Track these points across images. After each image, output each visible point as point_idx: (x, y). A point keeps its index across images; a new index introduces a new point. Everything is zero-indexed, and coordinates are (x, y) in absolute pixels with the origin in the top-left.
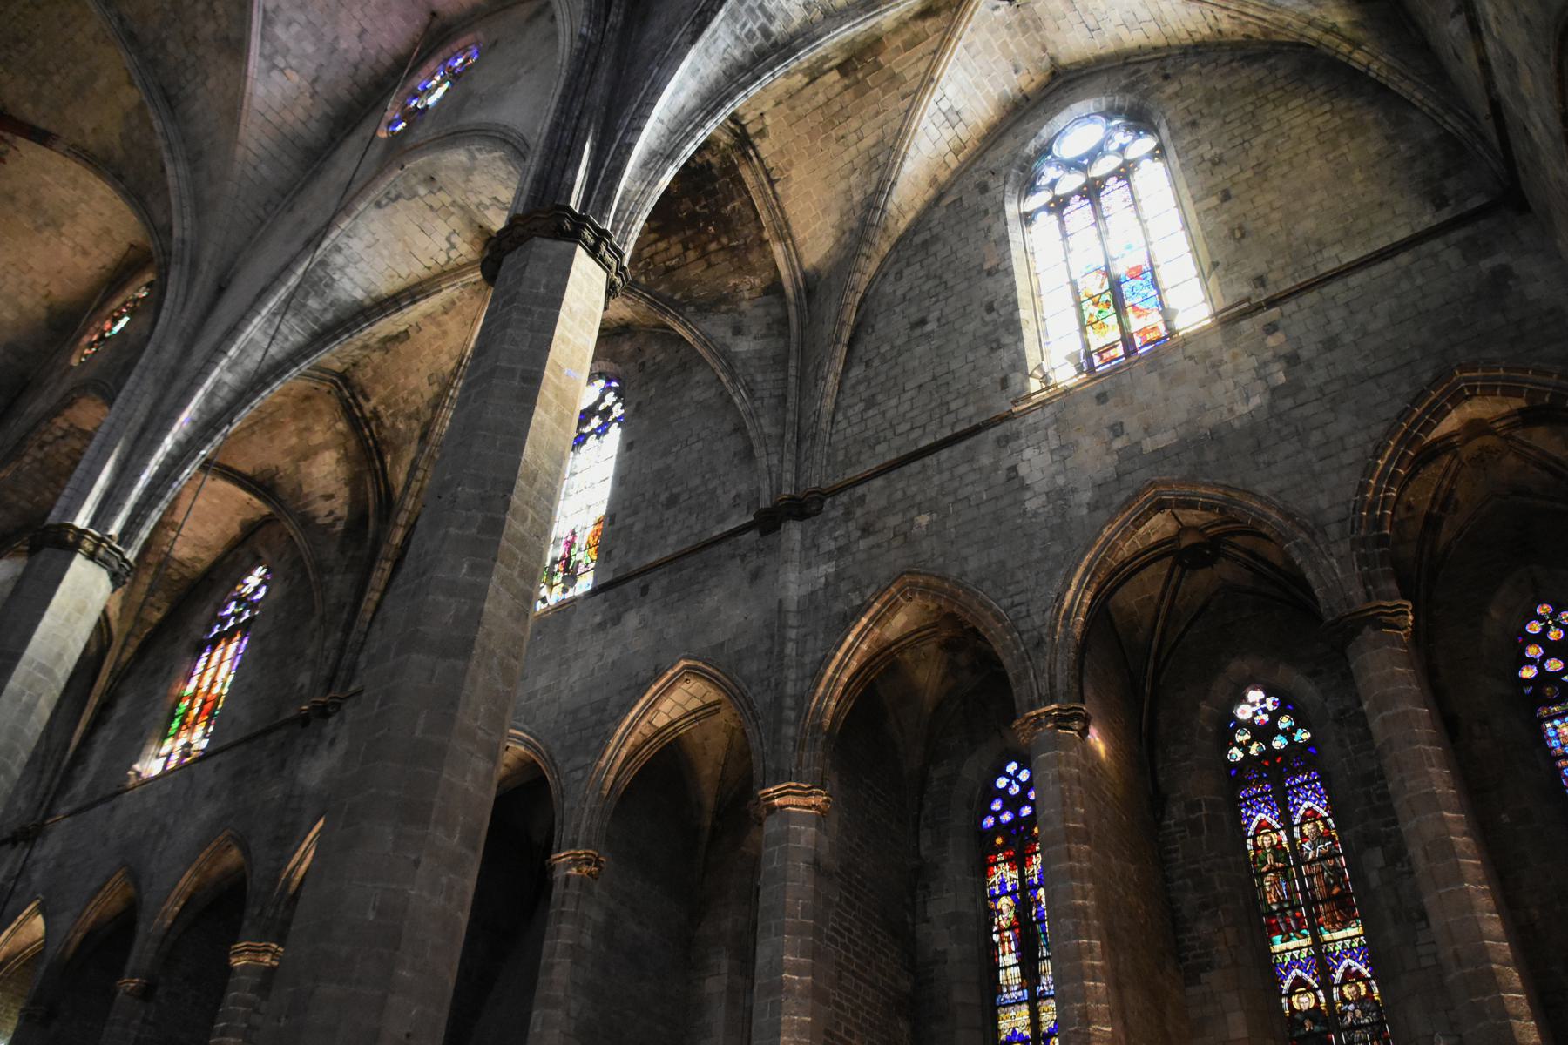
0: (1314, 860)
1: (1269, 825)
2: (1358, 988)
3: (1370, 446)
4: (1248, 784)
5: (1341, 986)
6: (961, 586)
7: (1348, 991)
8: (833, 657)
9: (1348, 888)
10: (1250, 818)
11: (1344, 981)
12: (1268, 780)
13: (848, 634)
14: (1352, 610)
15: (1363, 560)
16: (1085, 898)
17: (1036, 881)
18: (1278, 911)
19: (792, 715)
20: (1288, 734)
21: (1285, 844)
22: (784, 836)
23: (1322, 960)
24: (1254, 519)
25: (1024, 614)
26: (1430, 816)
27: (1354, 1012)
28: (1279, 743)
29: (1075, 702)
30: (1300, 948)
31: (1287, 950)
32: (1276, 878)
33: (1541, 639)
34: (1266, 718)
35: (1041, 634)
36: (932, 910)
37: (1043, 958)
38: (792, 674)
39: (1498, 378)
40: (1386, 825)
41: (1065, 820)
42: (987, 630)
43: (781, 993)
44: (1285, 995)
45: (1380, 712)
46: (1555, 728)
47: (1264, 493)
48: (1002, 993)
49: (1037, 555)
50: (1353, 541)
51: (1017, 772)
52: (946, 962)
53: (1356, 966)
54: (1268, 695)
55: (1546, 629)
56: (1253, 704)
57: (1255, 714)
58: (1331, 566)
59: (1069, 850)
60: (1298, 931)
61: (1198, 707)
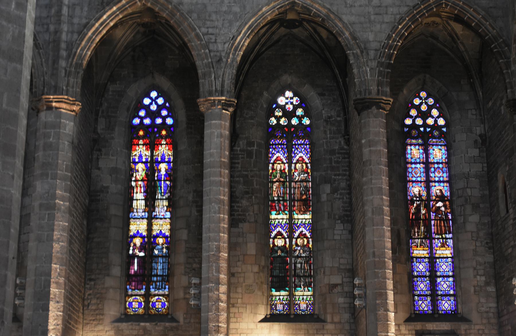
0: (297, 181)
1: (281, 160)
2: (304, 241)
3: (398, 17)
4: (276, 137)
5: (297, 239)
6: (179, 11)
7: (299, 241)
8: (93, 25)
9: (309, 197)
10: (273, 154)
11: (299, 237)
12: (286, 138)
13: (104, 13)
14: (370, 97)
15: (380, 73)
16: (224, 196)
17: (159, 159)
18: (277, 200)
19: (64, 53)
20: (300, 118)
21: (286, 171)
22: (57, 126)
23: (291, 226)
24: (337, 32)
25: (213, 40)
26: (378, 196)
27: (300, 250)
28: (295, 121)
29: (232, 97)
30: (283, 219)
31: (277, 219)
32: (279, 185)
33: (418, 108)
34: (291, 107)
35: (221, 56)
36: (101, 164)
37: (158, 199)
38: (65, 27)
39: (458, 5)
40: (335, 175)
41: (221, 157)
42: (189, 41)
43: (55, 210)
44: (272, 238)
45: (370, 147)
46: (411, 150)
47: (346, 21)
48: (133, 212)
49: (225, 9)
50: (378, 62)
51: (157, 98)
52: (108, 192)
53: (305, 232)
54: (295, 95)
55: (421, 104)
56: (287, 98)
57: (287, 103)
58: (367, 71)
59: (220, 172)
60: (284, 211)
61: (263, 94)
